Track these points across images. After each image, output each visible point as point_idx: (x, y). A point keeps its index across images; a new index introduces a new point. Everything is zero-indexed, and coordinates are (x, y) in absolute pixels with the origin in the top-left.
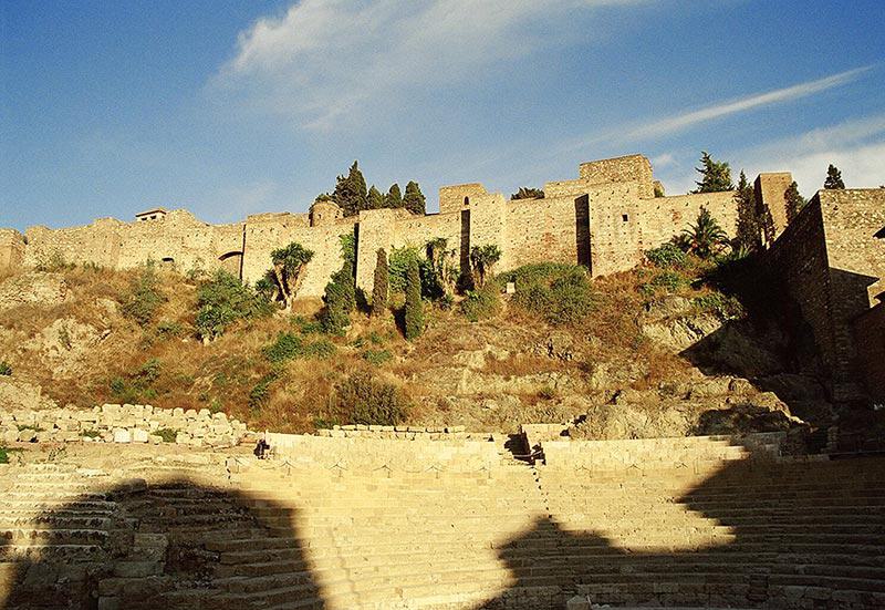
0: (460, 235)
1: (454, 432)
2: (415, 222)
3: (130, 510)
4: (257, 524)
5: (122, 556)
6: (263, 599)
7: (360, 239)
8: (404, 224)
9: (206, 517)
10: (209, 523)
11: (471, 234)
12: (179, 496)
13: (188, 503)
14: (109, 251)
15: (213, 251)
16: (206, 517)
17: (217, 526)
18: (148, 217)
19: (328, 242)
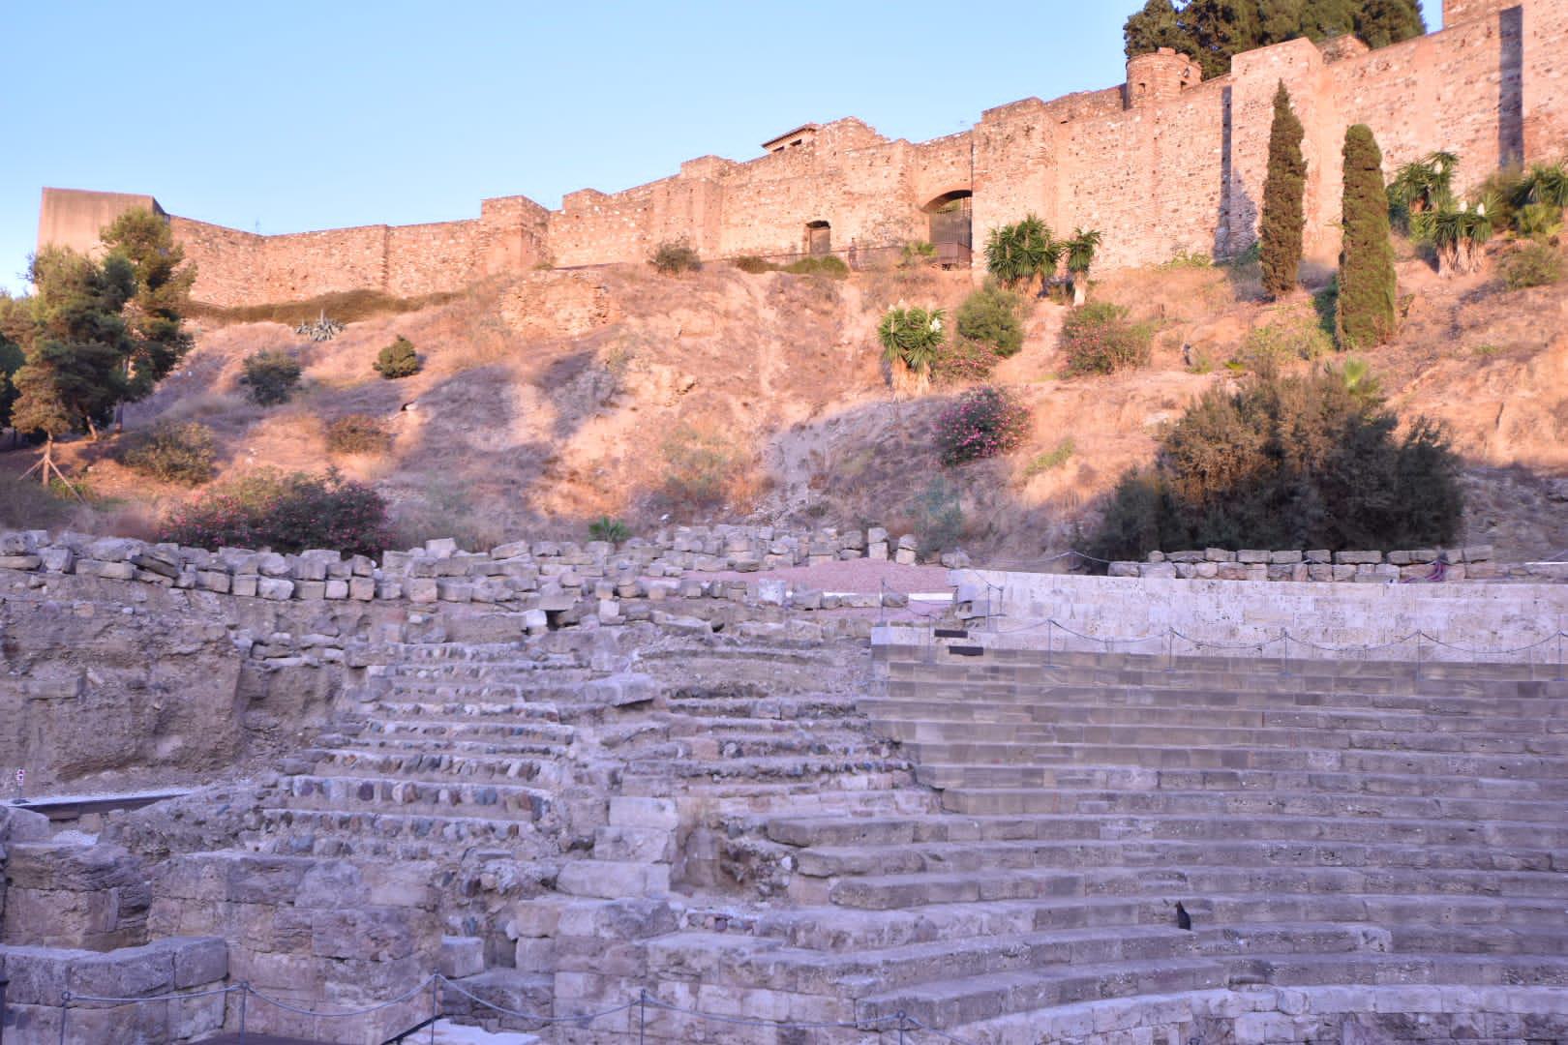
0: (1496, 76)
1: (1463, 561)
2: (1372, 60)
3: (610, 744)
4: (915, 777)
5: (584, 847)
6: (870, 970)
7: (1235, 122)
8: (1341, 70)
9: (787, 762)
10: (793, 776)
11: (1526, 65)
12: (744, 712)
13: (759, 729)
14: (698, 216)
15: (908, 195)
16: (787, 762)
17: (817, 784)
18: (787, 144)
19: (1160, 143)
